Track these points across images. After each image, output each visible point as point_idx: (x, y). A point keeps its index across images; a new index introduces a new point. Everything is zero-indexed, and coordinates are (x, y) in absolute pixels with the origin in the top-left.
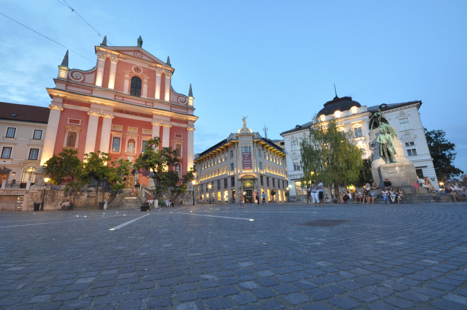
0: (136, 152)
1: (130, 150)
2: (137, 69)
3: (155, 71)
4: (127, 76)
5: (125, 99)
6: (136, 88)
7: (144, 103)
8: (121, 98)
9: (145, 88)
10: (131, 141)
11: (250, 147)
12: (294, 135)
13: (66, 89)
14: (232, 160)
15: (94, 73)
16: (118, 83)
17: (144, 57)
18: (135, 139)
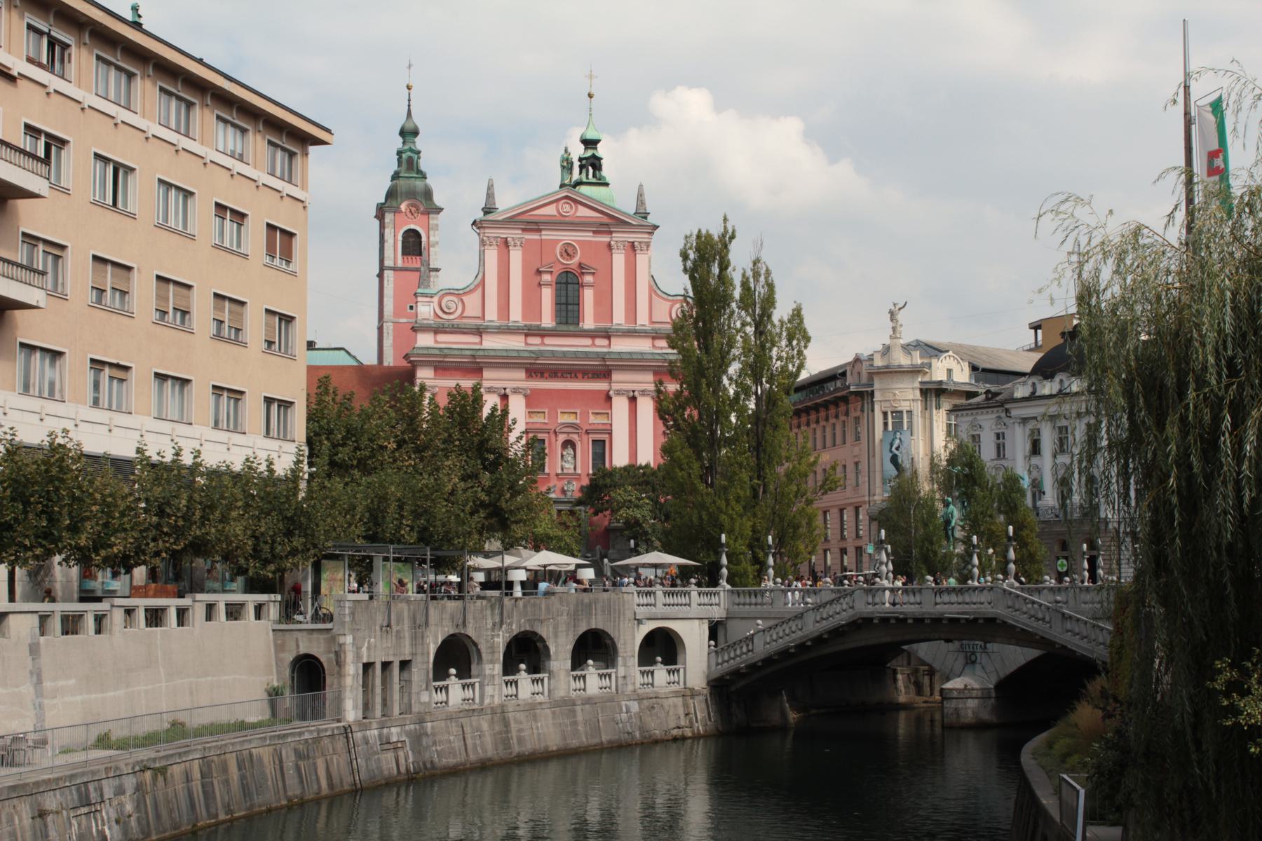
0: (579, 471)
1: (567, 465)
2: (568, 252)
3: (609, 246)
5: (548, 341)
6: (567, 304)
7: (588, 341)
8: (537, 340)
9: (588, 296)
10: (568, 444)
11: (910, 412)
12: (979, 417)
13: (436, 342)
14: (856, 450)
15: (479, 291)
16: (532, 304)
17: (583, 212)
18: (575, 437)
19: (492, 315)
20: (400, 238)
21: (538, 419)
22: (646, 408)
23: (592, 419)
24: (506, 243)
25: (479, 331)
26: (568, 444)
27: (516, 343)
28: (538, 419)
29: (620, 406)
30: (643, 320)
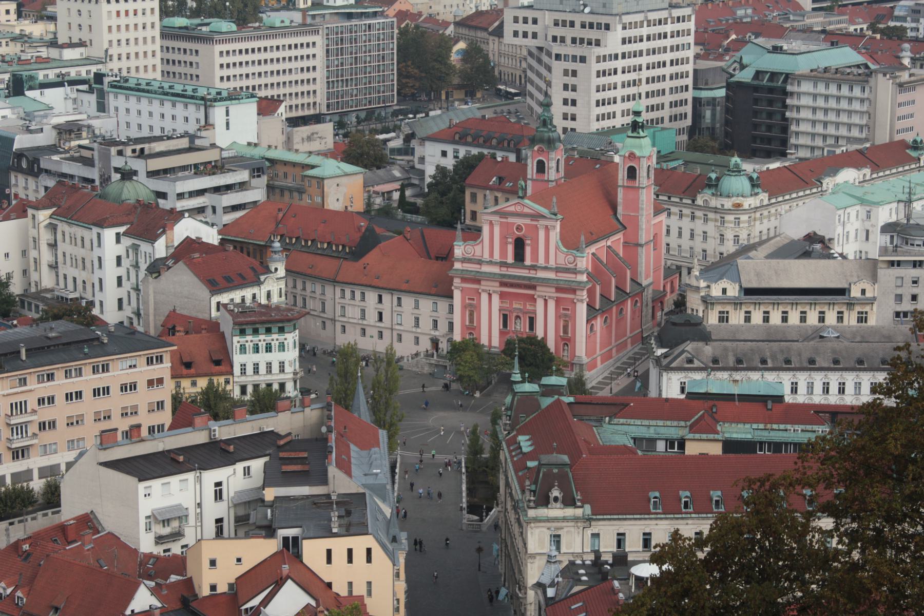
2: (519, 228)
4: (510, 240)
8: (505, 269)
9: (528, 250)
10: (518, 317)
16: (503, 252)
18: (521, 315)
19: (486, 256)
20: (535, 164)
21: (504, 305)
22: (552, 305)
23: (528, 307)
24: (491, 222)
25: (480, 262)
26: (518, 317)
27: (496, 270)
28: (504, 305)
29: (540, 304)
30: (552, 263)
